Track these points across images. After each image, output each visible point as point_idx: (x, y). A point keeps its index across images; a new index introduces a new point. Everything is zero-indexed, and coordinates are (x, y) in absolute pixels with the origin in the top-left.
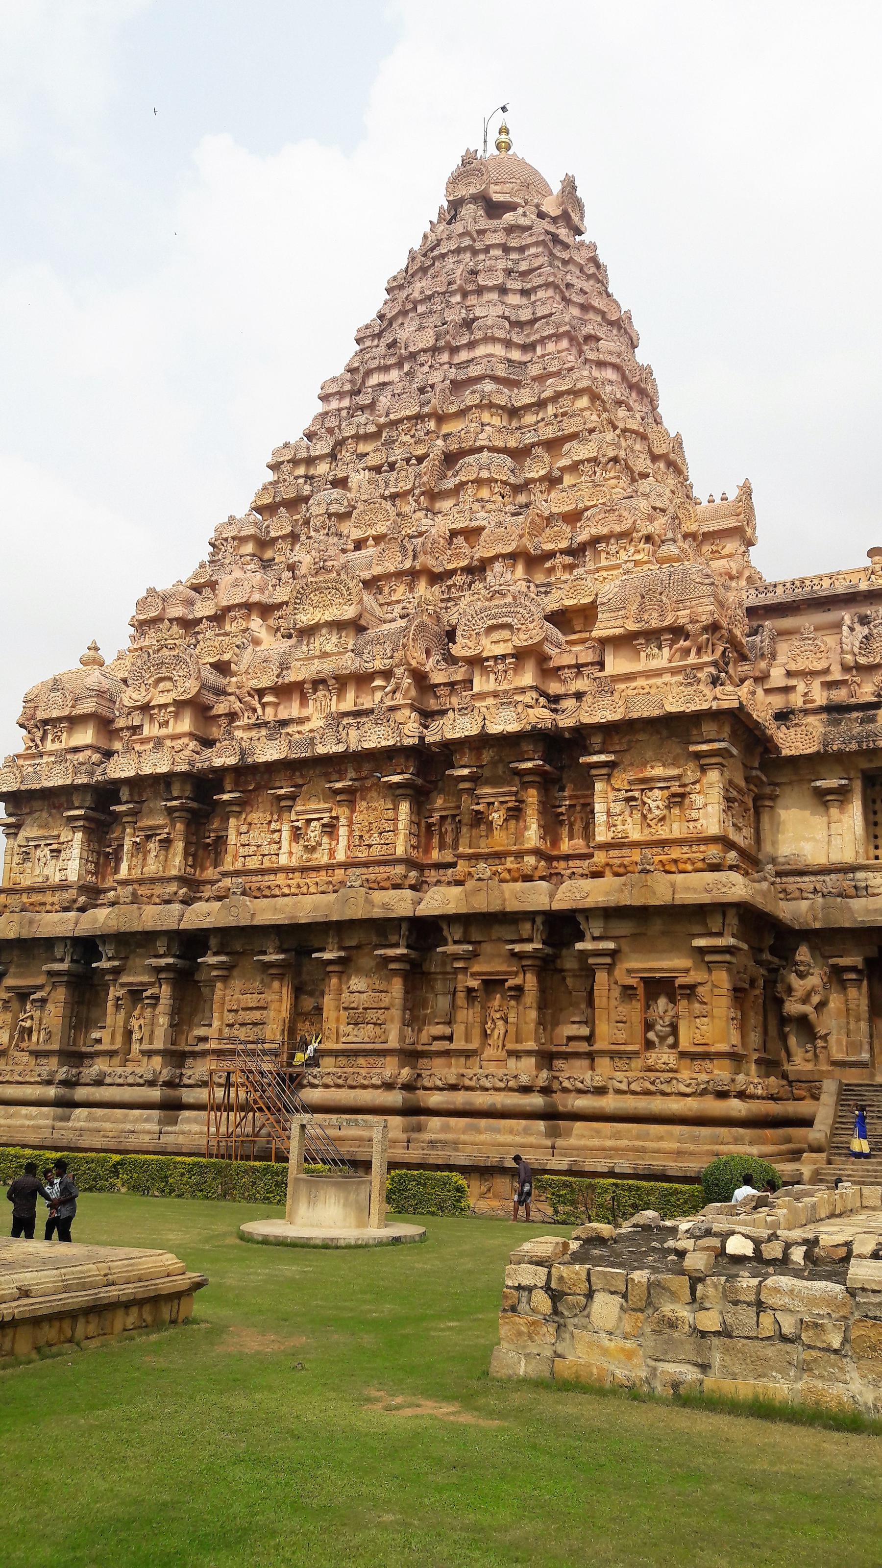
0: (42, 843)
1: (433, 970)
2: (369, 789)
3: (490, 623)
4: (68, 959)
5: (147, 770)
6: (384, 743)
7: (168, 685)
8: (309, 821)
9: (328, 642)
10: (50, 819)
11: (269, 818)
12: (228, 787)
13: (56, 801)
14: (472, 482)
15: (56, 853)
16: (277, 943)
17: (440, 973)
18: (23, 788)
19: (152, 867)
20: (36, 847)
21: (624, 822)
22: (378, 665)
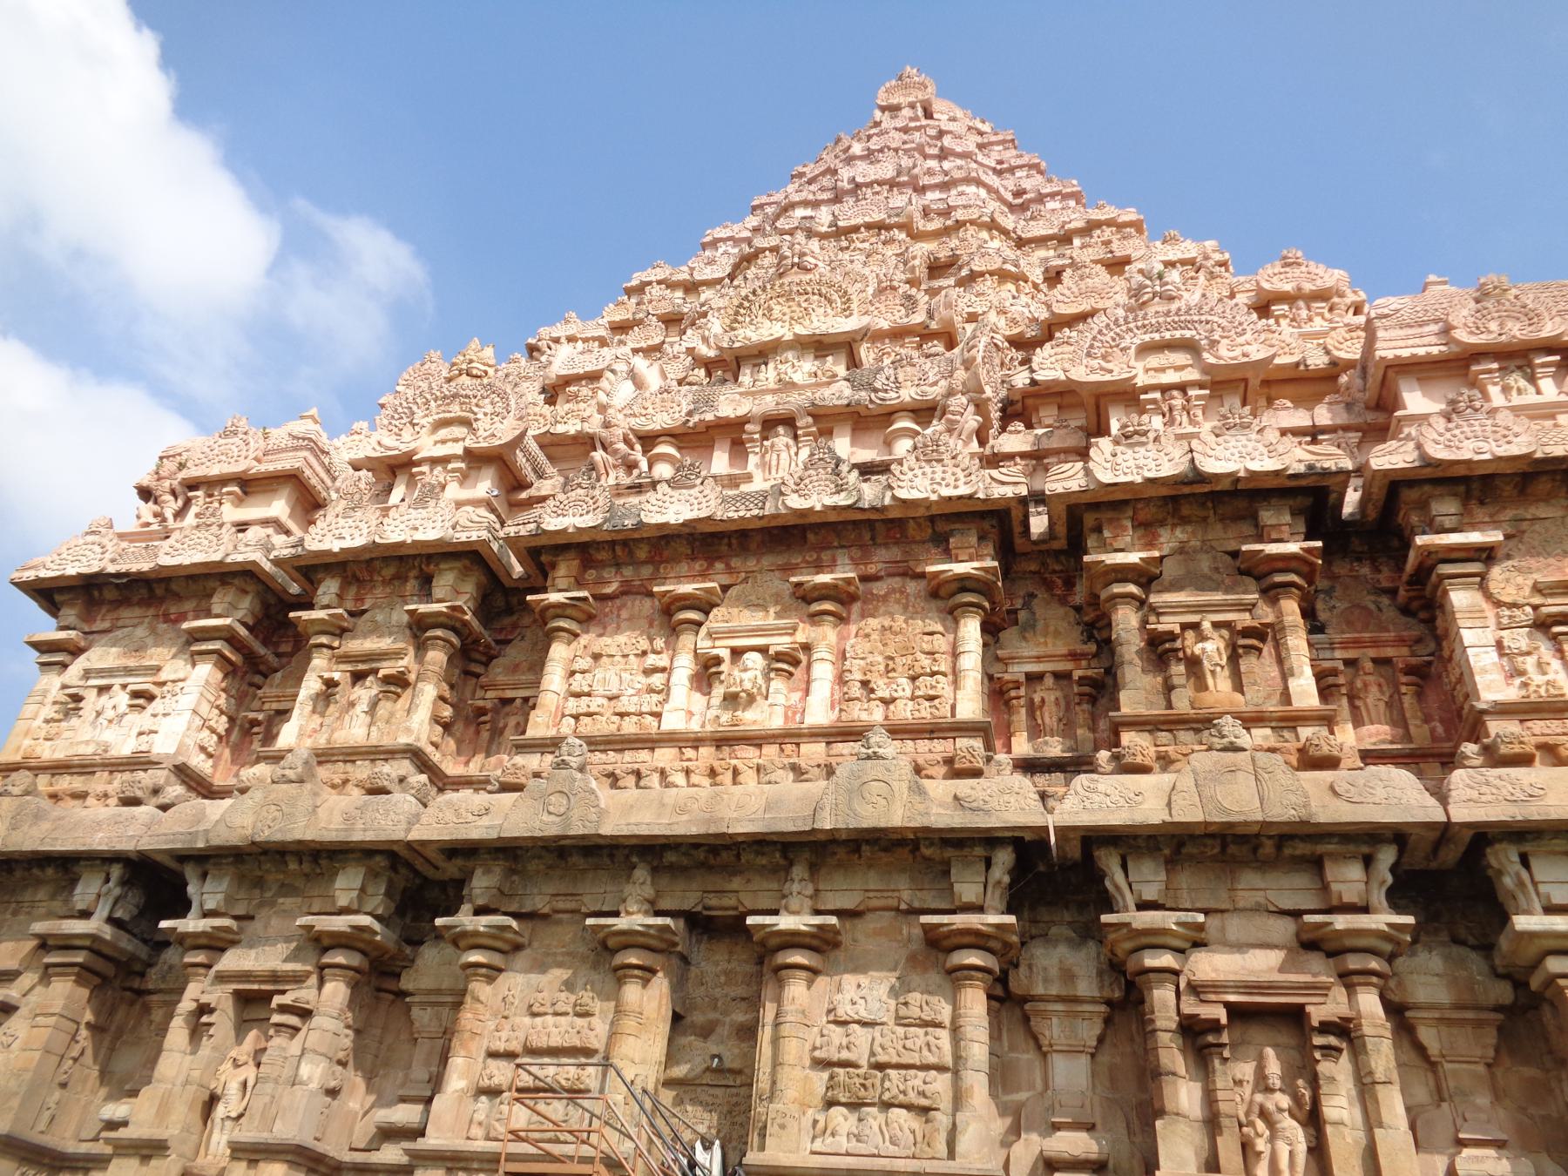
0: (117, 681)
1: (1039, 990)
2: (885, 598)
3: (1147, 338)
4: (102, 912)
6: (947, 492)
8: (737, 653)
9: (802, 369)
10: (150, 641)
12: (561, 583)
13: (173, 610)
14: (992, 274)
15: (143, 697)
16: (649, 891)
17: (1060, 999)
18: (111, 569)
19: (355, 731)
21: (1541, 667)
22: (908, 394)
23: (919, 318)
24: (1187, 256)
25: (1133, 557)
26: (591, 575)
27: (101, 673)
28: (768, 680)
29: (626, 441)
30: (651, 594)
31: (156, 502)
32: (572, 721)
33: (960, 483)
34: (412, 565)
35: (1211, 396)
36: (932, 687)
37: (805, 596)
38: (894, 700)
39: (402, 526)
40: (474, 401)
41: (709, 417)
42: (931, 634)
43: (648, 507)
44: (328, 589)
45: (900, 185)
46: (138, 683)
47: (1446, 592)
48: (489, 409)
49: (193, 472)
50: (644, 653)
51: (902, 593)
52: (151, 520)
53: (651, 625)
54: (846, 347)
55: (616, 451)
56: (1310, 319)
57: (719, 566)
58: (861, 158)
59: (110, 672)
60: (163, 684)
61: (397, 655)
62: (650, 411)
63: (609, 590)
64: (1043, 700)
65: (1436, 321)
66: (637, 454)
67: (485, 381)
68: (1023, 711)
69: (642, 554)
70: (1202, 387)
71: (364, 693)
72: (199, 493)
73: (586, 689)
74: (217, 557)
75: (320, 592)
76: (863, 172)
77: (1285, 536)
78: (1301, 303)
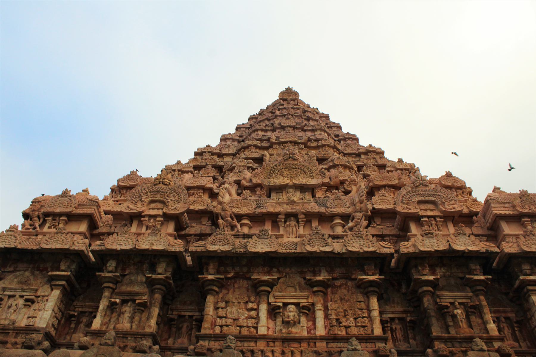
0: (18, 294)
2: (340, 287)
3: (420, 198)
5: (144, 245)
6: (366, 249)
7: (159, 205)
8: (286, 305)
9: (297, 196)
10: (32, 278)
11: (246, 299)
12: (211, 271)
13: (42, 266)
14: (342, 165)
18: (19, 247)
19: (125, 325)
20: (10, 297)
23: (327, 180)
24: (406, 167)
25: (431, 278)
26: (222, 269)
27: (10, 289)
28: (300, 316)
29: (231, 217)
30: (250, 279)
31: (31, 220)
32: (220, 328)
33: (370, 246)
34: (147, 259)
35: (444, 221)
36: (364, 322)
37: (311, 284)
38: (350, 327)
39: (147, 242)
40: (166, 194)
41: (264, 211)
42: (360, 302)
43: (250, 245)
44: (111, 265)
45: (297, 128)
46: (28, 295)
47: (530, 296)
48: (173, 198)
49: (49, 210)
50: (247, 302)
51: (346, 285)
52: (29, 227)
53: (248, 291)
54: (311, 190)
55: (227, 220)
56: (457, 195)
57: (275, 270)
58: (279, 116)
59: (15, 290)
60: (39, 297)
61: (143, 294)
62: (239, 206)
63: (230, 276)
64: (396, 328)
65: (509, 203)
66: (235, 222)
67: (169, 187)
68: (389, 332)
69: (244, 262)
70: (441, 218)
71: (128, 310)
72: (50, 218)
73: (225, 315)
74: (66, 247)
75: (108, 265)
76: (284, 122)
77: (478, 273)
78: (454, 190)
